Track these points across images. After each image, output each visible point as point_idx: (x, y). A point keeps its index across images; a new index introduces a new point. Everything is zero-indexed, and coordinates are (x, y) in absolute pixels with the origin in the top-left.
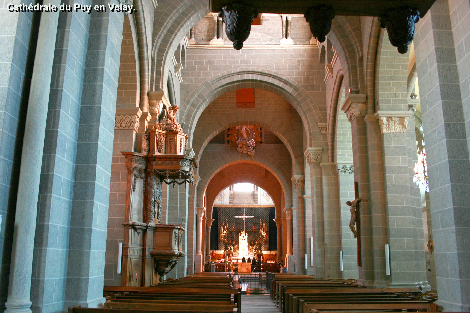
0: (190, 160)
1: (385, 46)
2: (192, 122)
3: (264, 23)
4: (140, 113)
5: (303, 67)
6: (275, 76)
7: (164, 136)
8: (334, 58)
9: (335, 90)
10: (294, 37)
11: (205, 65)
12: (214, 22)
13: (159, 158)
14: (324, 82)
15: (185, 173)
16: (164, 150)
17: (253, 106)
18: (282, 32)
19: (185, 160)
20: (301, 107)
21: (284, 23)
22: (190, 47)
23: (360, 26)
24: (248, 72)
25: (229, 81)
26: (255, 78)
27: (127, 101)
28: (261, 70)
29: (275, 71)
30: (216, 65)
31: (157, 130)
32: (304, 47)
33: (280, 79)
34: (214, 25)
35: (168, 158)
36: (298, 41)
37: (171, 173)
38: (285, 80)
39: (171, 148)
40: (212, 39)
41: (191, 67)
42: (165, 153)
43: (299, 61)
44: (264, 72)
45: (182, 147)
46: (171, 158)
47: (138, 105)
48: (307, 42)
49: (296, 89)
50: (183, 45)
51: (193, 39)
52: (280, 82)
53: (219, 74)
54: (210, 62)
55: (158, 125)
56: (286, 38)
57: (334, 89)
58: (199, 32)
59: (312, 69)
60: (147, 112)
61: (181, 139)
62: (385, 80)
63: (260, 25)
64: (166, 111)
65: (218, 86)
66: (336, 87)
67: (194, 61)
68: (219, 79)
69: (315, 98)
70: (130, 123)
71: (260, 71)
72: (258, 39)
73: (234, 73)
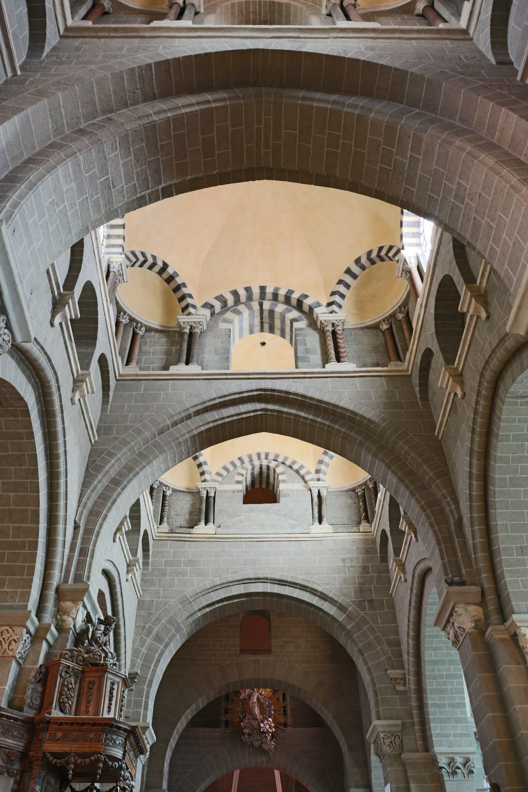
0: (125, 730)
1: (501, 492)
3: (282, 500)
4: (33, 623)
5: (351, 569)
7: (77, 677)
8: (406, 544)
9: (413, 604)
10: (334, 521)
11: (182, 567)
12: (201, 498)
14: (391, 595)
15: (110, 763)
17: (269, 651)
18: (313, 514)
19: (115, 729)
20: (354, 641)
21: (316, 500)
23: (448, 469)
24: (258, 580)
25: (223, 596)
27: (11, 597)
29: (303, 577)
30: (201, 567)
31: (63, 661)
32: (350, 536)
34: (201, 504)
35: (78, 724)
37: (79, 761)
38: (321, 593)
39: (88, 702)
40: (197, 525)
41: (159, 570)
42: (76, 714)
45: (113, 702)
46: (83, 724)
47: (32, 604)
48: (355, 529)
49: (342, 608)
50: (146, 532)
51: (165, 524)
52: (313, 597)
53: (207, 582)
56: (320, 521)
57: (410, 602)
58: (176, 515)
59: (366, 573)
60: (50, 622)
62: (513, 555)
63: (276, 504)
64: (91, 630)
66: (414, 598)
67: (164, 560)
69: (378, 623)
70: (8, 642)
71: (277, 577)
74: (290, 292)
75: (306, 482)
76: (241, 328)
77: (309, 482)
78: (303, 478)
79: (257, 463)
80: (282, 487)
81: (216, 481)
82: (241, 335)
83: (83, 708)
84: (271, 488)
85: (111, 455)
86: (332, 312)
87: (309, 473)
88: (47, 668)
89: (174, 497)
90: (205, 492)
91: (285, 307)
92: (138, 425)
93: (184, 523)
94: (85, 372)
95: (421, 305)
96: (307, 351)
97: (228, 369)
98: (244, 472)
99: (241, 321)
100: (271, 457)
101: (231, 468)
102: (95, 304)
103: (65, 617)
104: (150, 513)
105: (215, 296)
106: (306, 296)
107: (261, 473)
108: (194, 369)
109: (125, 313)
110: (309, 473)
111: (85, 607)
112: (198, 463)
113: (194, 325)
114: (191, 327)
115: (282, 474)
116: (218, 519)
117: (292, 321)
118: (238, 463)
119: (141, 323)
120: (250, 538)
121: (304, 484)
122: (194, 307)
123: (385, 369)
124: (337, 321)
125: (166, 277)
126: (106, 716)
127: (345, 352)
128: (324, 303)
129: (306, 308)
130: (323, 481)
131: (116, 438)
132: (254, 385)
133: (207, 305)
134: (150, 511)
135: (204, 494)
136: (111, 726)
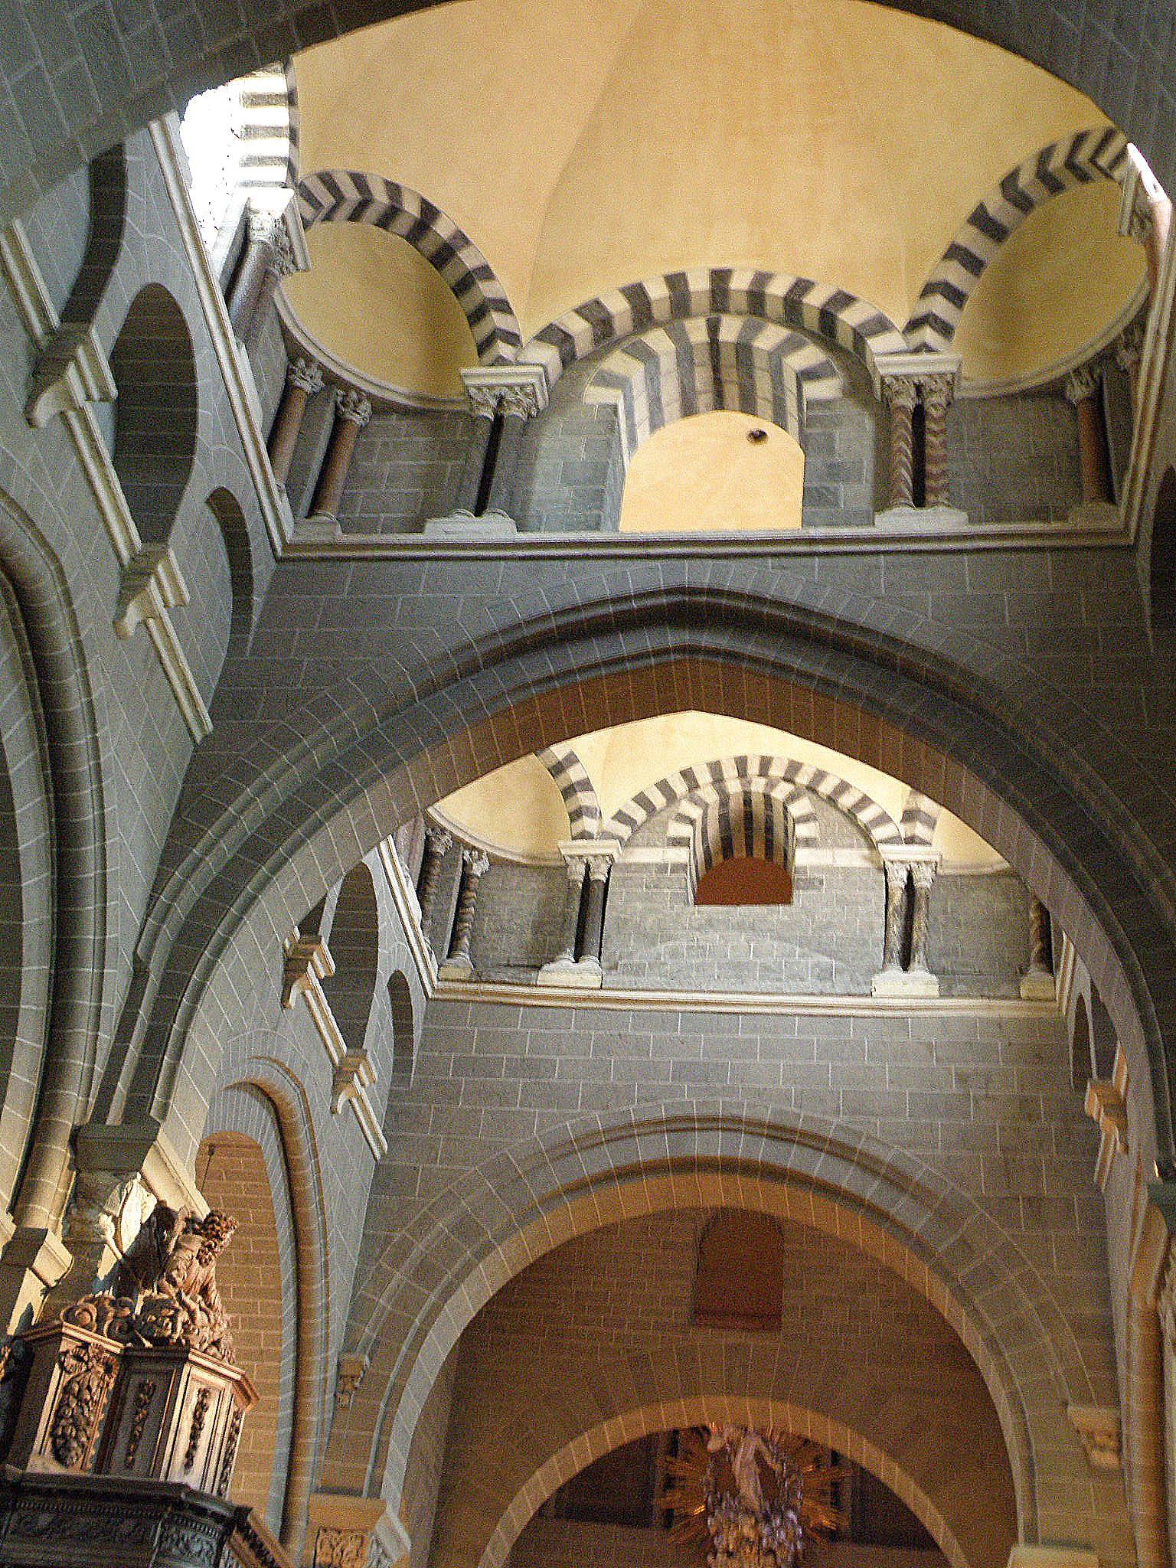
2: (410, 1362)
3: (799, 896)
6: (842, 1146)
7: (108, 1370)
12: (570, 885)
13: (46, 1490)
16: (93, 1452)
21: (898, 897)
22: (443, 991)
24: (710, 1123)
26: (740, 1154)
28: (774, 1112)
29: (843, 1119)
31: (69, 1329)
32: (989, 1008)
33: (868, 1165)
34: (568, 902)
36: (961, 981)
39: (134, 1439)
43: (962, 1079)
44: (788, 1123)
45: (203, 1442)
48: (1005, 989)
51: (463, 957)
54: (527, 1067)
55: (92, 1308)
61: (204, 1393)
65: (559, 1183)
68: (564, 1150)
71: (768, 1116)
72: (766, 968)
73: (640, 1124)
74: (802, 286)
75: (872, 846)
76: (655, 403)
77: (881, 847)
78: (865, 833)
79: (734, 786)
80: (802, 858)
81: (613, 837)
82: (656, 423)
83: (119, 1454)
84: (778, 859)
85: (245, 774)
86: (917, 351)
87: (884, 819)
88: (28, 1346)
89: (494, 882)
90: (582, 869)
91: (784, 333)
92: (327, 691)
93: (517, 955)
94: (156, 547)
95: (1158, 332)
96: (834, 471)
97: (597, 527)
98: (695, 813)
99: (653, 379)
100: (777, 771)
101: (658, 800)
102: (184, 349)
103: (88, 1215)
104: (413, 926)
105: (578, 303)
106: (845, 300)
107: (748, 816)
108: (496, 527)
109: (309, 360)
110: (884, 819)
111: (150, 1189)
112: (565, 785)
113: (510, 396)
114: (501, 399)
115: (805, 819)
116: (610, 948)
117: (807, 375)
118: (680, 787)
119: (359, 390)
120: (697, 1003)
121: (866, 852)
122: (512, 339)
123: (1055, 526)
124: (930, 376)
125: (433, 249)
126: (176, 1478)
127: (944, 473)
128: (900, 322)
129: (845, 339)
130: (924, 842)
131: (265, 727)
132: (659, 576)
133: (553, 335)
134: (411, 920)
135: (578, 873)
136: (179, 1505)
